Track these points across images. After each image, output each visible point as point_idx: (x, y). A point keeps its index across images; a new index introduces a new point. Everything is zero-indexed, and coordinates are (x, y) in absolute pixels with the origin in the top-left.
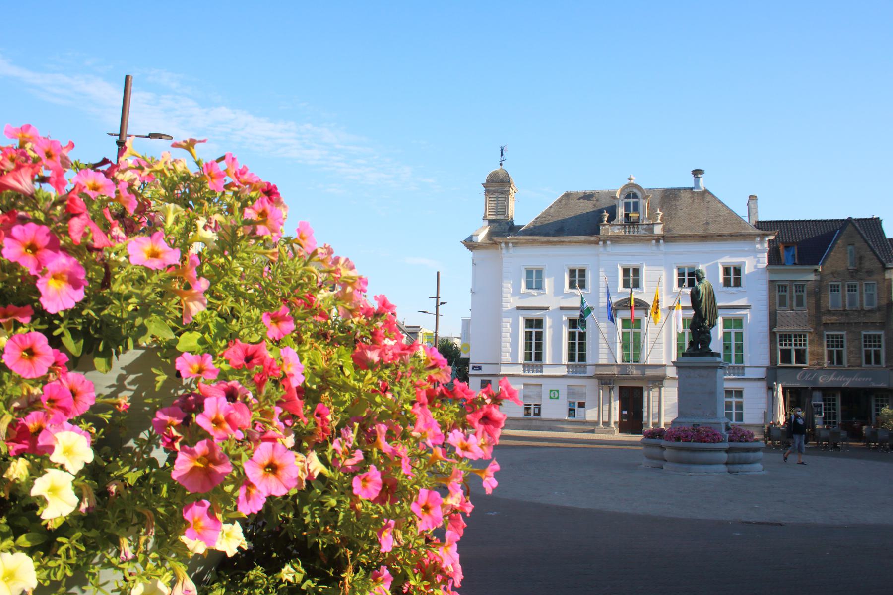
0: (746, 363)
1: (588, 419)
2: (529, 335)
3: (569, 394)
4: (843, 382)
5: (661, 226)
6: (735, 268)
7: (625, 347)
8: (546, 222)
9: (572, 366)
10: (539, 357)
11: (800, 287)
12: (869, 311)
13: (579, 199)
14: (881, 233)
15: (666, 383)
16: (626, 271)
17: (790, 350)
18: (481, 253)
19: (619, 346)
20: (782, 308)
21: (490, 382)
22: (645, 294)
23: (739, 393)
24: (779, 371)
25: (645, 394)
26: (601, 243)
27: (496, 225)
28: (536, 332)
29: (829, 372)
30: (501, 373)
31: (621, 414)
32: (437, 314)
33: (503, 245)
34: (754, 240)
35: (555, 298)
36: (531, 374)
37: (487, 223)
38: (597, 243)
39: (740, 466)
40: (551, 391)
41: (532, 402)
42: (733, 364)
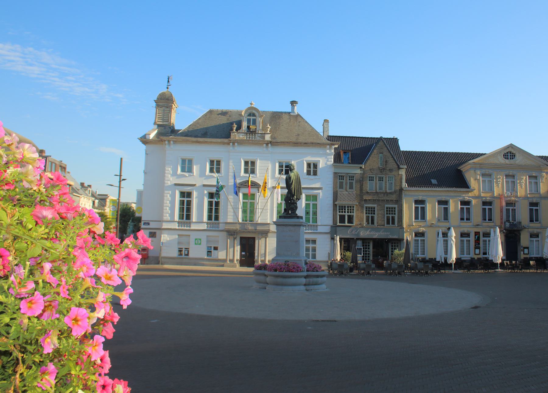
0: (319, 223)
1: (220, 257)
2: (182, 203)
3: (208, 241)
4: (374, 235)
5: (270, 135)
6: (314, 164)
7: (244, 211)
8: (196, 128)
9: (210, 223)
10: (188, 217)
11: (352, 178)
12: (390, 193)
13: (218, 115)
14: (398, 147)
15: (269, 235)
16: (246, 163)
17: (344, 216)
18: (152, 147)
19: (240, 210)
20: (341, 190)
21: (155, 233)
22: (258, 178)
23: (314, 242)
24: (338, 228)
25: (257, 242)
26: (231, 144)
27: (163, 128)
28: (187, 201)
29: (366, 229)
30: (163, 227)
31: (241, 255)
32: (120, 187)
33: (167, 142)
34: (326, 147)
35: (200, 178)
36: (183, 228)
37: (156, 126)
38: (228, 144)
39: (313, 286)
40: (196, 239)
41: (183, 247)
42: (311, 223)
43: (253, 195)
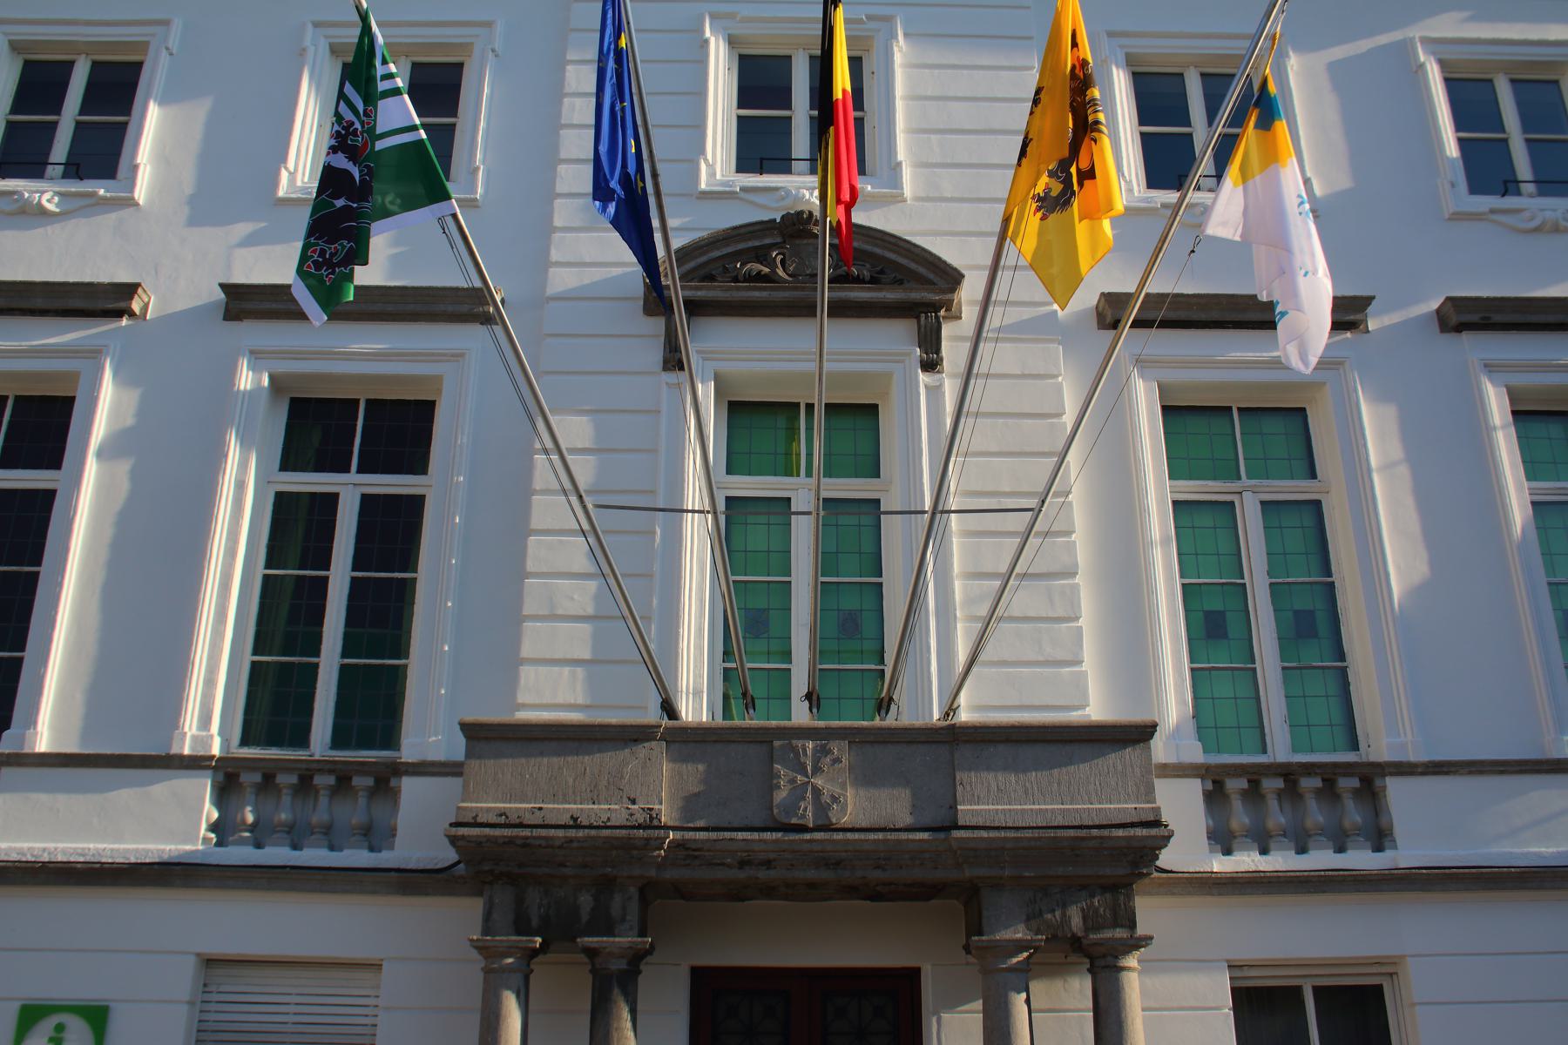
9: (268, 777)
43: (857, 421)
